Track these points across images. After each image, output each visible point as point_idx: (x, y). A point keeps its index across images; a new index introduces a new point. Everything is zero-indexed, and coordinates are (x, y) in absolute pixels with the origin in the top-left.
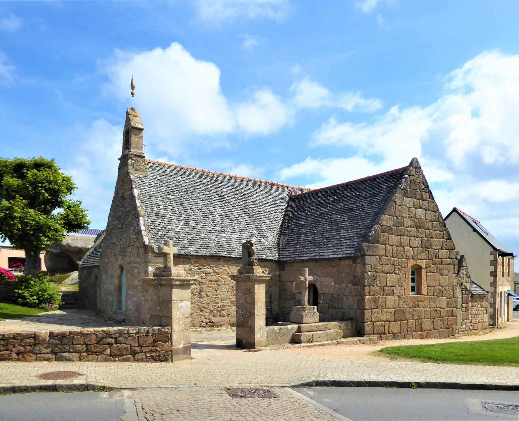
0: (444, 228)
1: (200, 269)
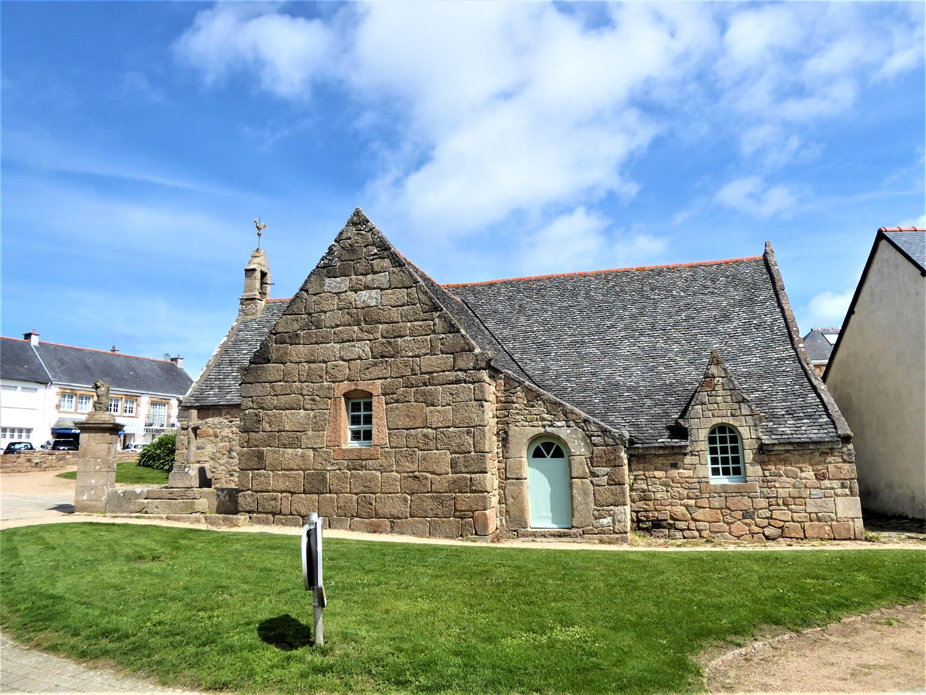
0: (436, 314)
1: (231, 422)
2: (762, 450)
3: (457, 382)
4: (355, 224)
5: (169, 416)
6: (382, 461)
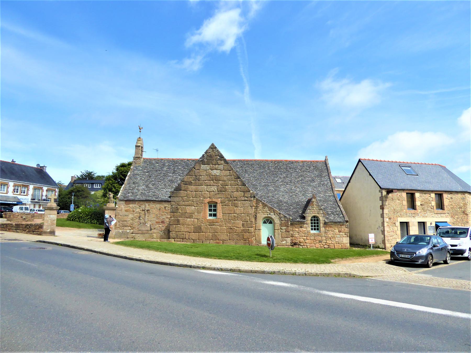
2: (325, 223)
3: (245, 200)
4: (212, 148)
5: (42, 196)
6: (220, 223)
